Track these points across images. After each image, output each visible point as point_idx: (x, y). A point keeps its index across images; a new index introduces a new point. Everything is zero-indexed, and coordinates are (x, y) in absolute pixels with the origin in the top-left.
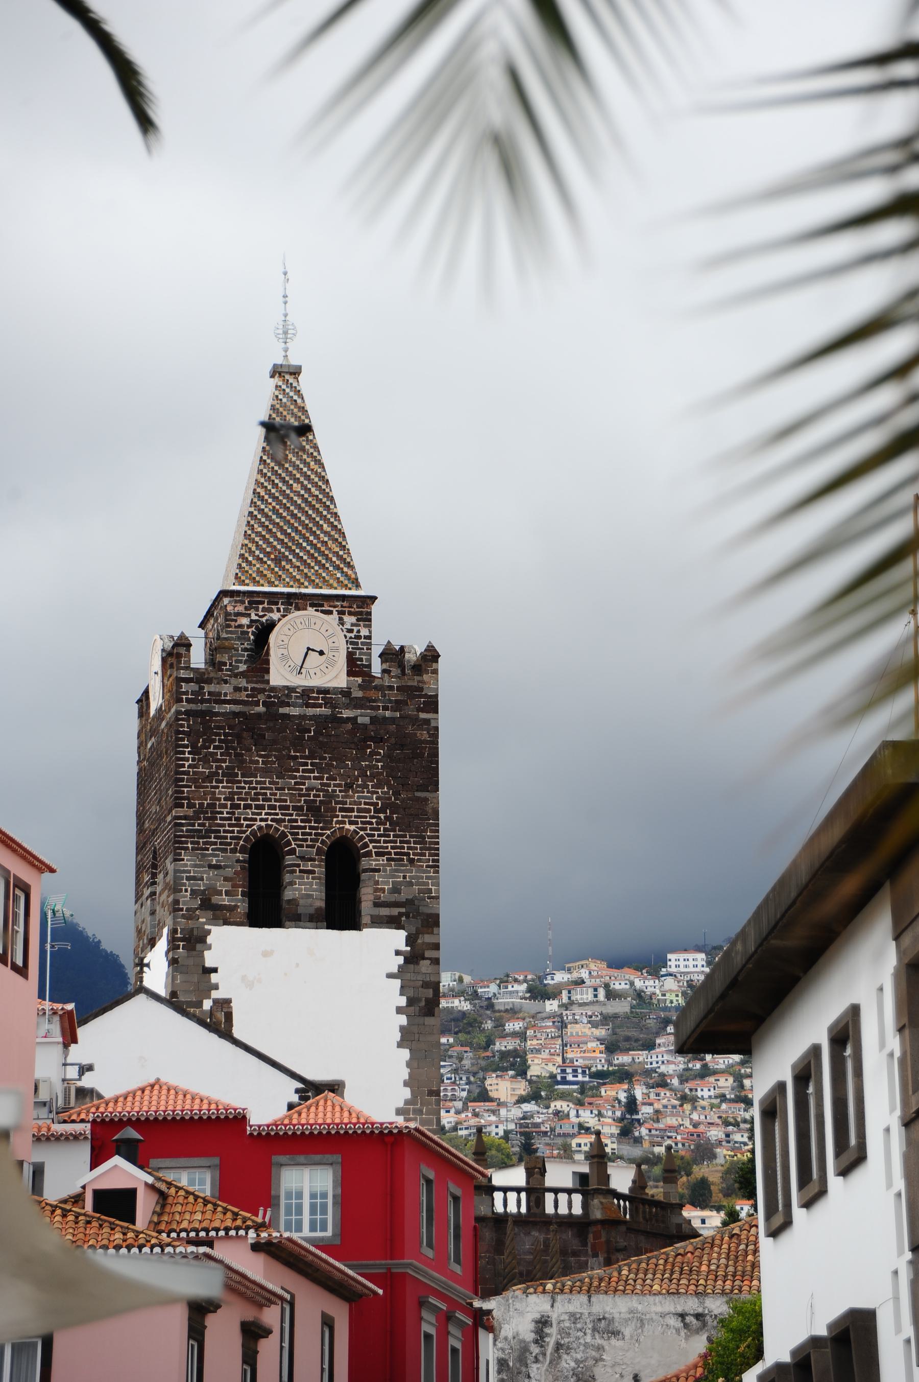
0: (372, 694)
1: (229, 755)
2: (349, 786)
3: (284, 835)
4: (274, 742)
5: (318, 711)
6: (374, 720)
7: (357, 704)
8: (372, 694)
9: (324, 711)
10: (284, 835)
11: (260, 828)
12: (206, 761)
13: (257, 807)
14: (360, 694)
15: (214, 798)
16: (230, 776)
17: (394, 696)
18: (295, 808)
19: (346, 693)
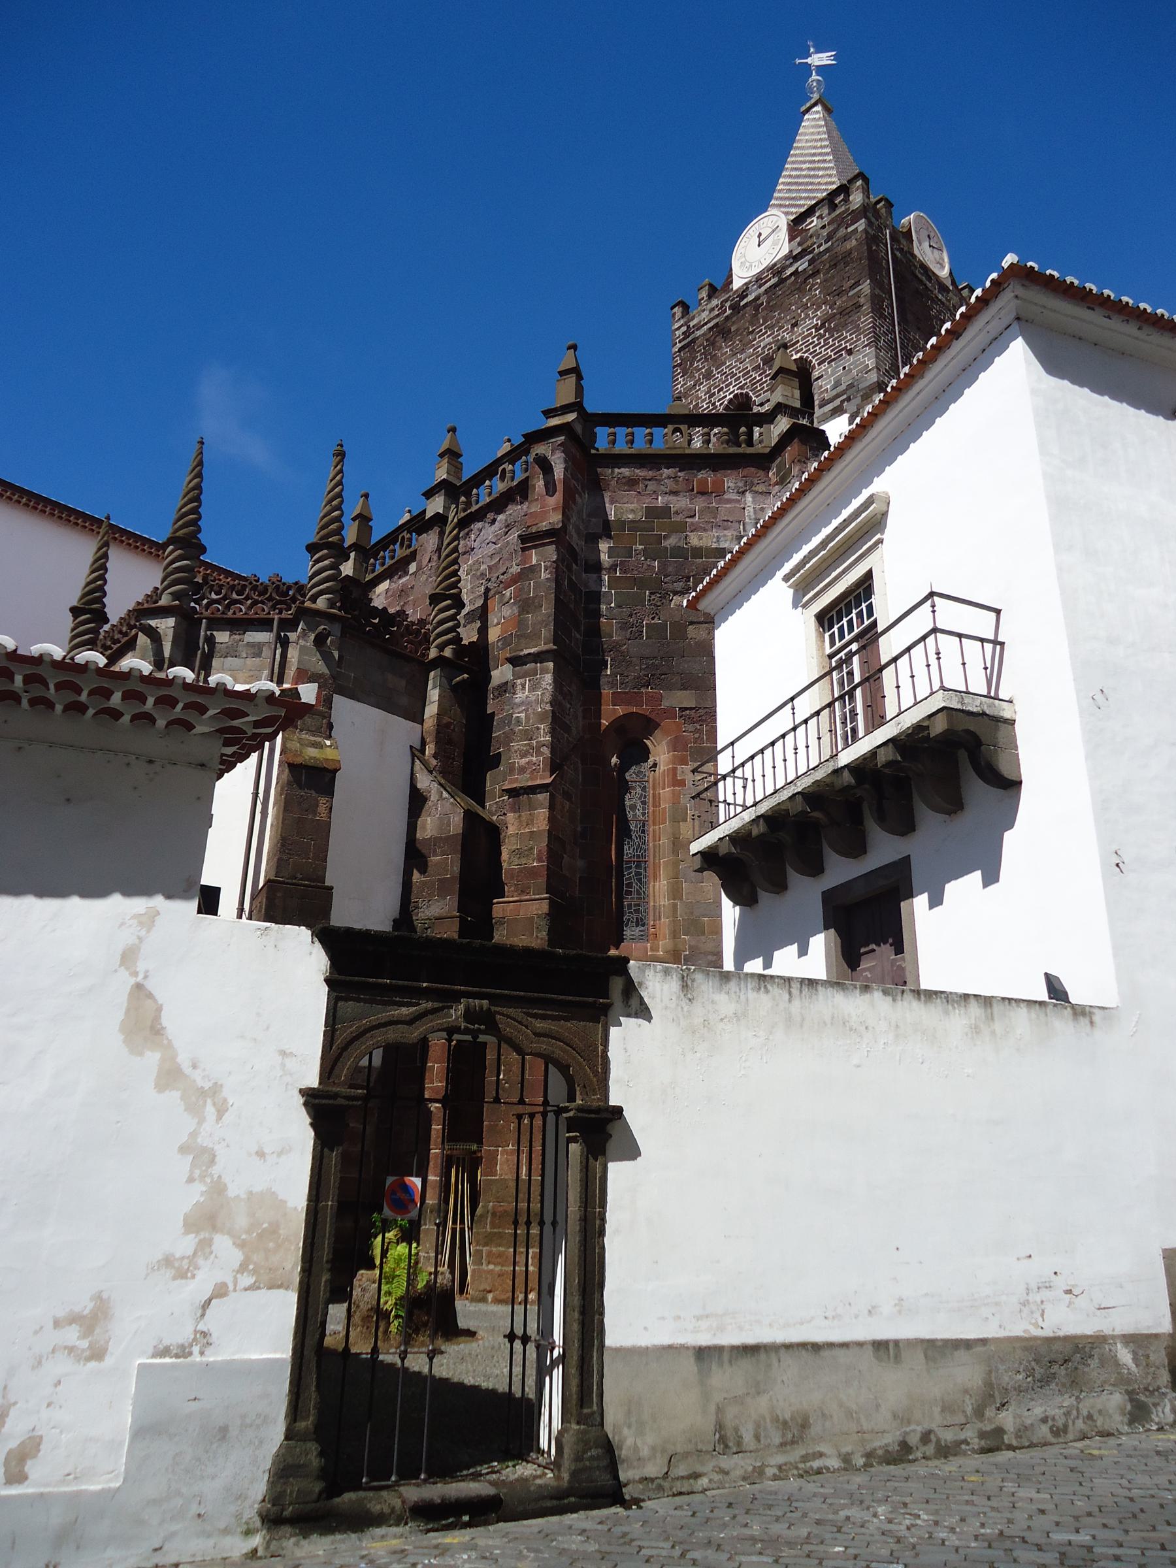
0: (809, 243)
1: (706, 360)
2: (795, 325)
3: (747, 394)
4: (738, 330)
5: (768, 285)
6: (811, 262)
7: (796, 258)
8: (809, 243)
9: (773, 281)
10: (747, 394)
11: (730, 401)
12: (692, 376)
13: (727, 386)
14: (800, 249)
15: (698, 398)
16: (708, 376)
17: (825, 233)
18: (753, 369)
19: (786, 257)
